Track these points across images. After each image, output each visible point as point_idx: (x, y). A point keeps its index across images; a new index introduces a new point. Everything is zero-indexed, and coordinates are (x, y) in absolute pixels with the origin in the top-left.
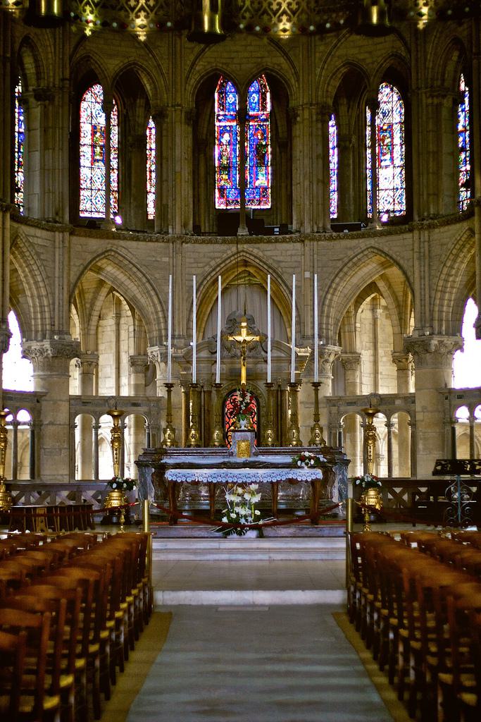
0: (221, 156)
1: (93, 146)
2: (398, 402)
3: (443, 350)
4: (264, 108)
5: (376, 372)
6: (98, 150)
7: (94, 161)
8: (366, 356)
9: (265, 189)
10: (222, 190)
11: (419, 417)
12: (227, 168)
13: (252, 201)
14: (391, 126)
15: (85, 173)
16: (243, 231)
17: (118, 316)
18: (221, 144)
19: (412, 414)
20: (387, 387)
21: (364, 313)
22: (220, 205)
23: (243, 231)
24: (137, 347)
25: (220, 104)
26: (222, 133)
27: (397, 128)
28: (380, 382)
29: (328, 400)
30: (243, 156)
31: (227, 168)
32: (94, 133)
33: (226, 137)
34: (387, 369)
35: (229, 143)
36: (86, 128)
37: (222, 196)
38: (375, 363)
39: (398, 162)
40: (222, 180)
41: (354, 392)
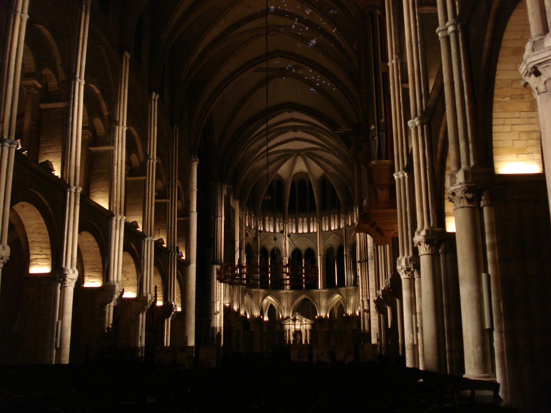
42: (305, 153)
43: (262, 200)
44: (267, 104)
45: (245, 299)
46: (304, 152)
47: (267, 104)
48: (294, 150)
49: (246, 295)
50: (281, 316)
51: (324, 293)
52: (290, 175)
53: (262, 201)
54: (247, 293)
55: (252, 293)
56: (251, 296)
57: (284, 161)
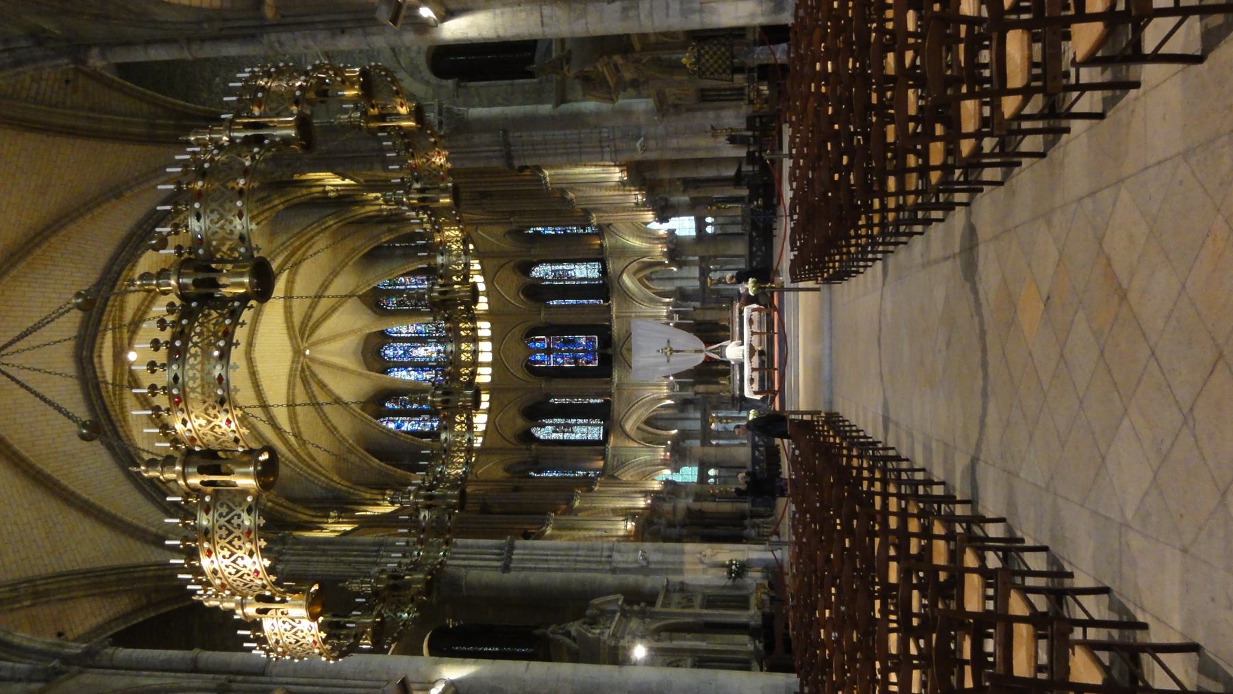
0: (569, 363)
1: (564, 432)
2: (703, 265)
3: (675, 241)
4: (543, 340)
5: (687, 278)
6: (566, 430)
7: (572, 432)
9: (587, 339)
10: (588, 362)
11: (711, 253)
12: (576, 360)
13: (593, 346)
14: (552, 271)
15: (578, 437)
16: (610, 351)
18: (563, 363)
19: (710, 257)
20: (695, 272)
22: (596, 364)
23: (610, 351)
25: (541, 363)
26: (557, 363)
28: (692, 276)
30: (569, 351)
31: (576, 360)
32: (557, 432)
33: (559, 360)
34: (686, 272)
35: (562, 358)
36: (555, 436)
37: (591, 362)
39: (572, 267)
40: (582, 362)
41: (698, 290)
42: (302, 338)
43: (414, 438)
44: (67, 415)
45: (630, 479)
46: (299, 340)
47: (67, 415)
48: (293, 362)
49: (619, 475)
50: (669, 402)
51: (619, 306)
52: (360, 374)
53: (417, 439)
54: (615, 475)
55: (615, 463)
56: (622, 464)
57: (323, 386)
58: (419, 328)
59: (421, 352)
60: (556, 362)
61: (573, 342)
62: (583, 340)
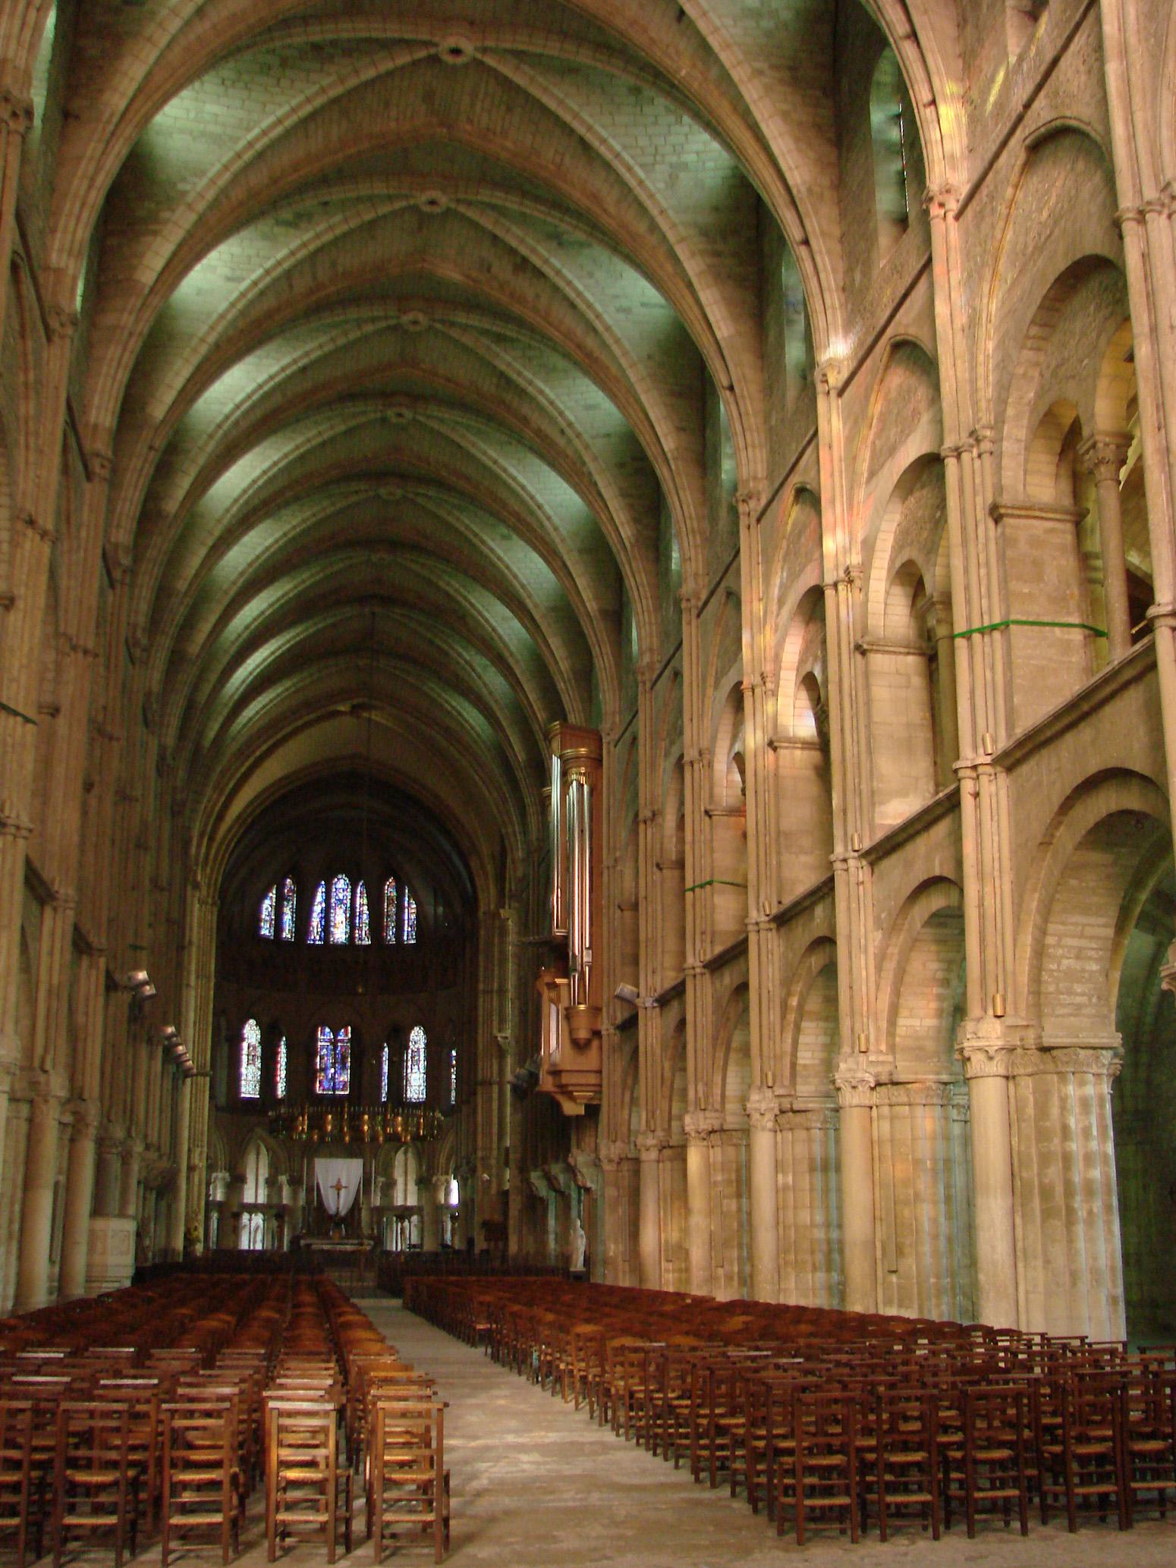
5: (406, 1191)
8: (400, 1181)
15: (243, 1070)
17: (258, 1154)
20: (412, 1201)
21: (400, 1157)
22: (318, 1090)
24: (270, 1174)
27: (422, 1051)
29: (377, 1209)
33: (324, 1051)
34: (412, 1188)
36: (245, 1045)
38: (406, 1184)
39: (422, 1070)
40: (321, 1076)
58: (365, 917)
59: (339, 917)
60: (322, 1047)
61: (344, 1067)
62: (345, 1077)
